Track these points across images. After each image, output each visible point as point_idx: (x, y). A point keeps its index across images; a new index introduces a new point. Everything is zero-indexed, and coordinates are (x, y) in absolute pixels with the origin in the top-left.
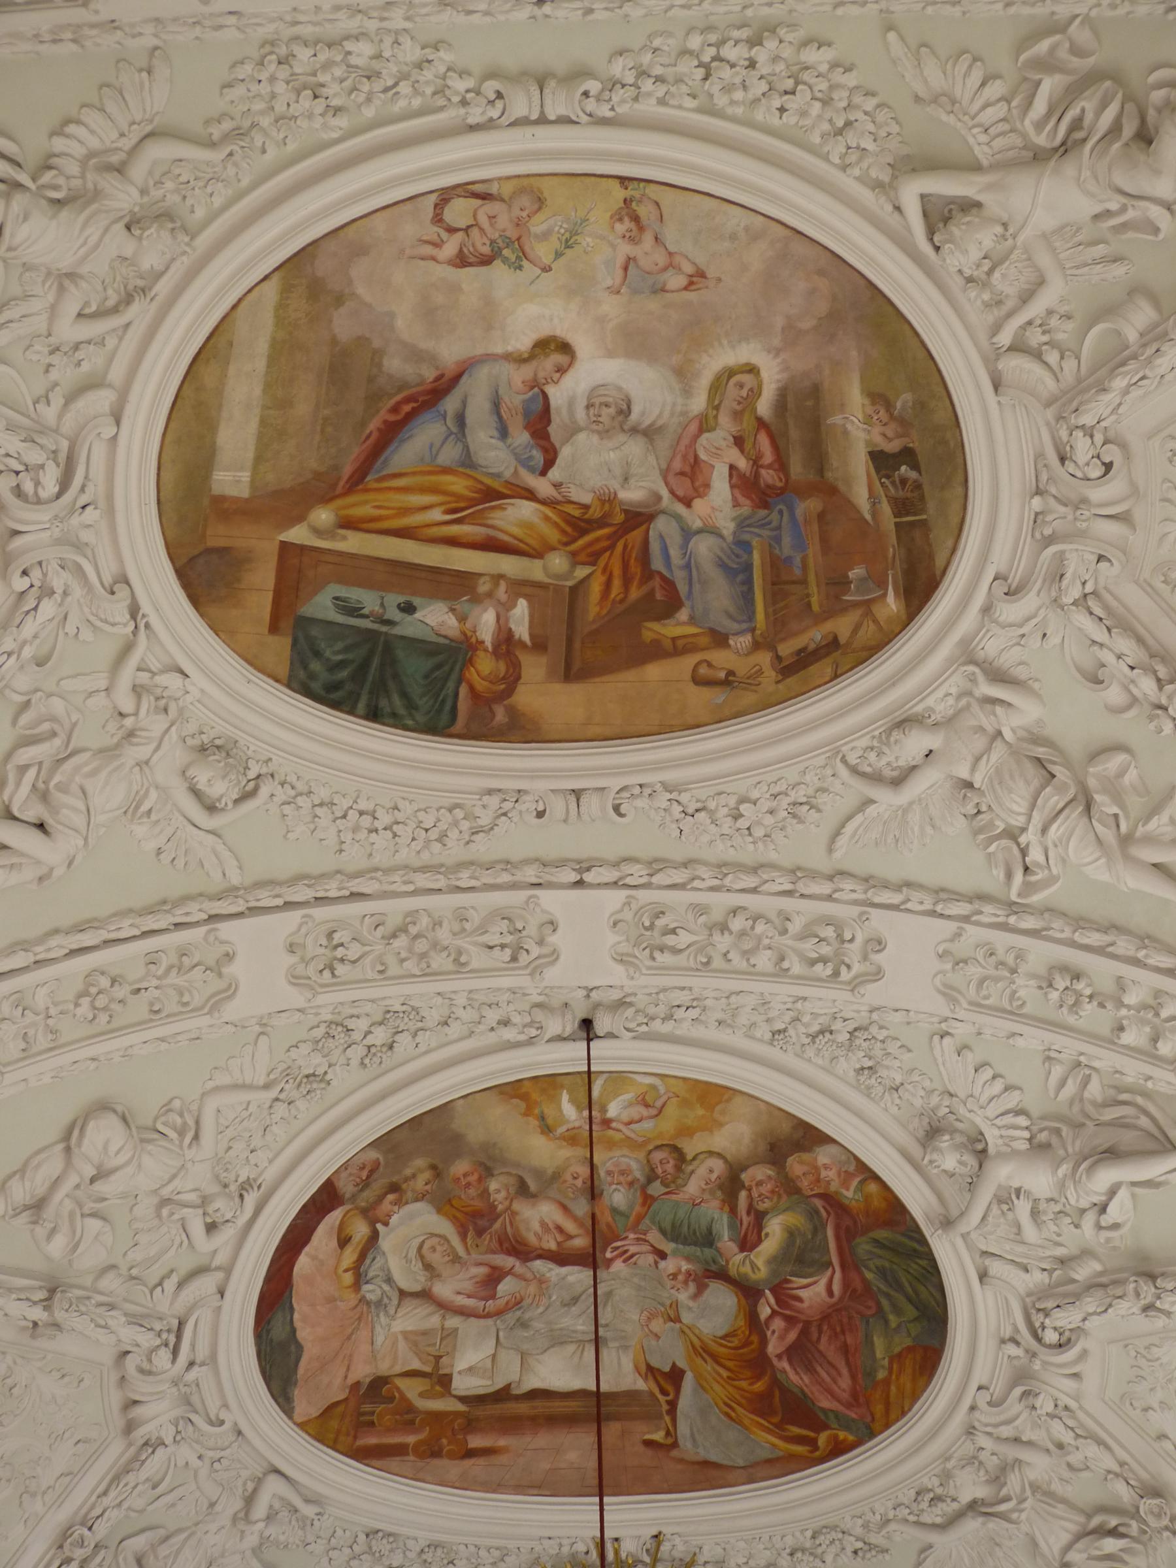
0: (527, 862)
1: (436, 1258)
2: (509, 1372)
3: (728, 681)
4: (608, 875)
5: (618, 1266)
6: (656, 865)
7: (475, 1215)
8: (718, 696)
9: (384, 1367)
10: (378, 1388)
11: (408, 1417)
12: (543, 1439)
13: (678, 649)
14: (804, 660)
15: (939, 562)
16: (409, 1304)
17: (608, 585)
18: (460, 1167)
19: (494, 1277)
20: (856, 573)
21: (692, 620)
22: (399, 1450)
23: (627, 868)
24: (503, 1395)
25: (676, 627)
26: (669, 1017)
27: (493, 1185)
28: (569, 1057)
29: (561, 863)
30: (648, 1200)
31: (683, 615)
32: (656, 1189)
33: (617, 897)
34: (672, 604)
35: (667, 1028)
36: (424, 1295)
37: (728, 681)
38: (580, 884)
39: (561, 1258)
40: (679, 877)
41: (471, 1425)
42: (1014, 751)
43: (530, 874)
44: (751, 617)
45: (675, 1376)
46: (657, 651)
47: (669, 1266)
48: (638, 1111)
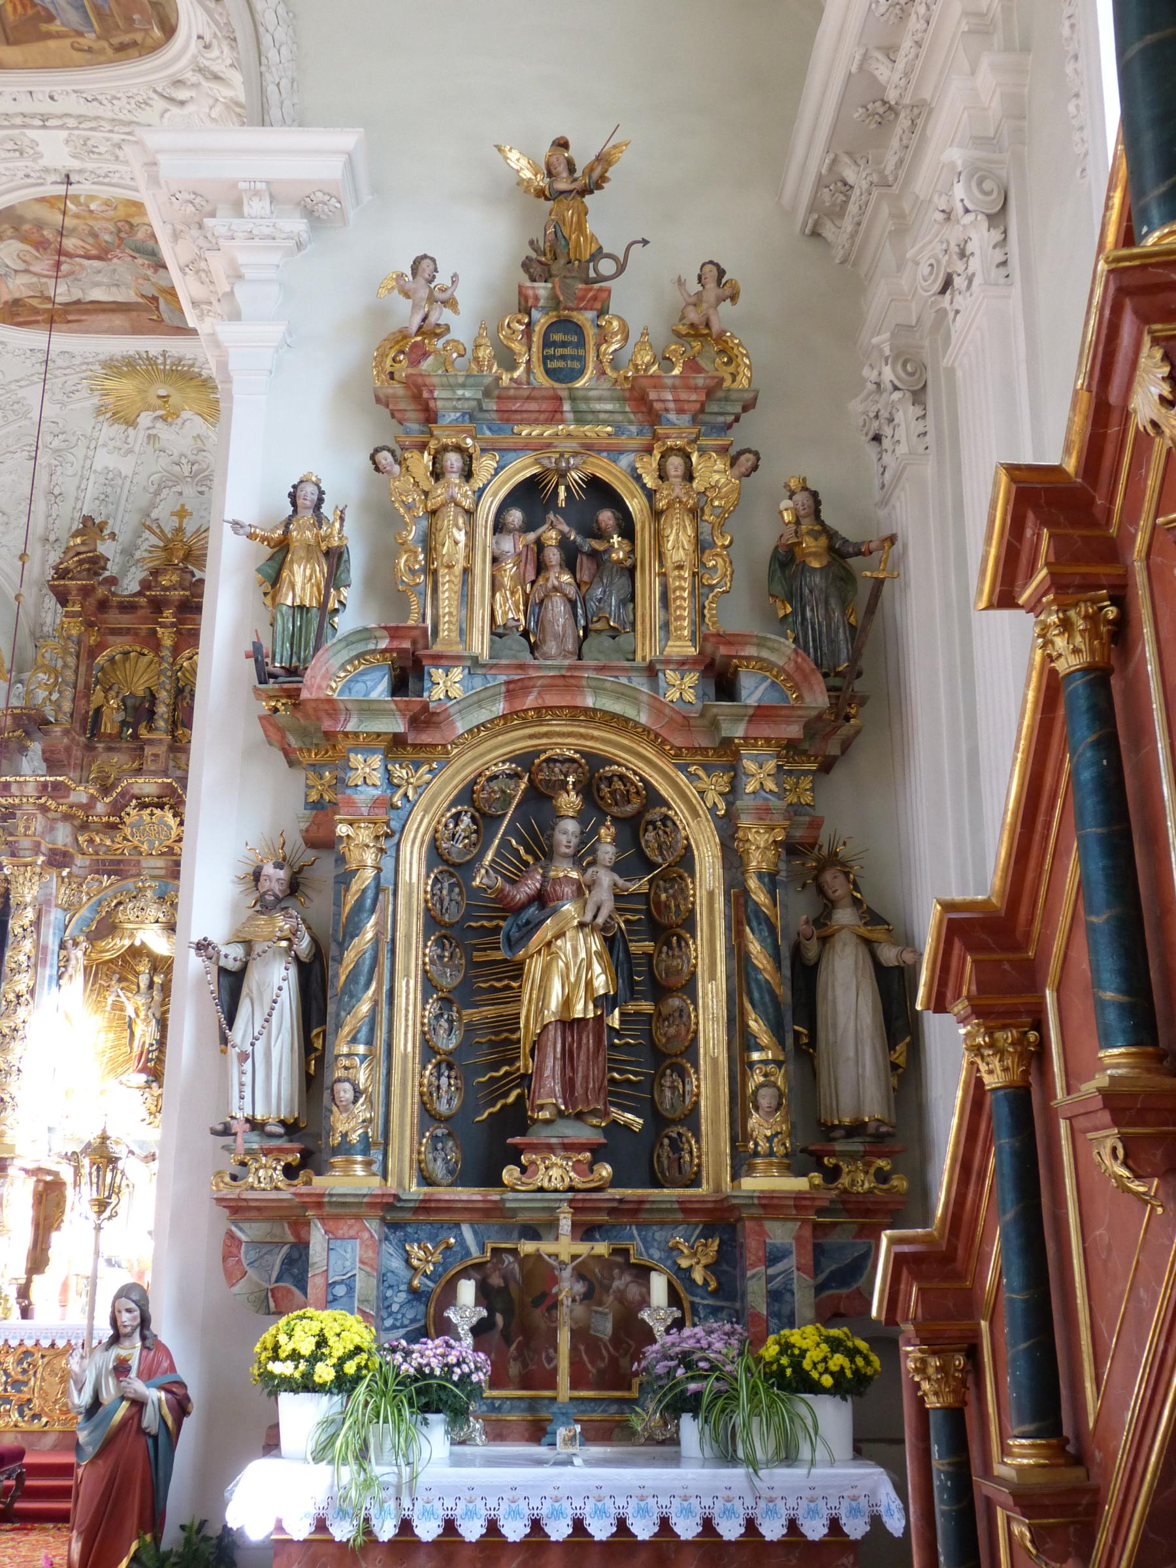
0: (16, 115)
1: (27, 258)
2: (77, 294)
3: (90, 50)
4: (59, 122)
5: (115, 260)
6: (81, 118)
7: (41, 243)
8: (88, 56)
9: (17, 295)
10: (16, 302)
11: (36, 311)
12: (102, 317)
13: (59, 36)
14: (122, 48)
15: (173, 21)
16: (20, 275)
17: (15, 8)
18: (26, 227)
19: (58, 265)
20: (136, 17)
21: (63, 24)
22: (37, 322)
23: (66, 120)
24: (78, 302)
25: (56, 26)
26: (106, 176)
27: (45, 233)
28: (61, 190)
29: (33, 116)
30: (121, 239)
31: (58, 22)
32: (123, 235)
33: (64, 134)
34: (50, 18)
35: (107, 180)
36: (27, 271)
37: (90, 50)
38: (44, 127)
39: (89, 258)
40: (93, 124)
41: (66, 312)
42: (227, 107)
43: (18, 121)
44: (92, 26)
45: (155, 299)
46: (49, 36)
47: (139, 261)
48: (104, 208)
